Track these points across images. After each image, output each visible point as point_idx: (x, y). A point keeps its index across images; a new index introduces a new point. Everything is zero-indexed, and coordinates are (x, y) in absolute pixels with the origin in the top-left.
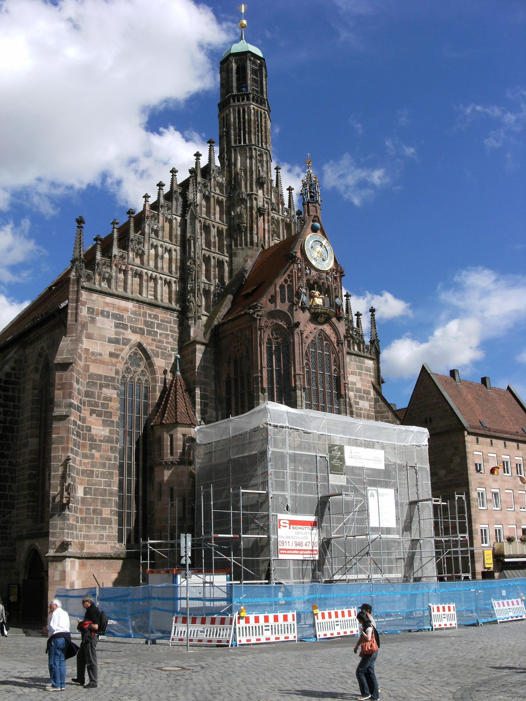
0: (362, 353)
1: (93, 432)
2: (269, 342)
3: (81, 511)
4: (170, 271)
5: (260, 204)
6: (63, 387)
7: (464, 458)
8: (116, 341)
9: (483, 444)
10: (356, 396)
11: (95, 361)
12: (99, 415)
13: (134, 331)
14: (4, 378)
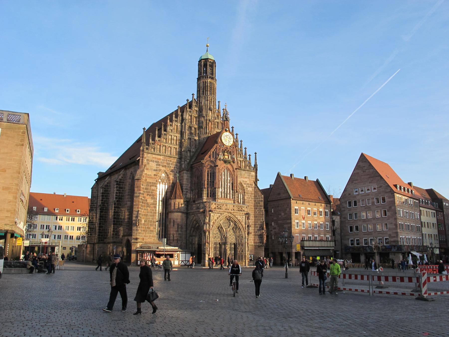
1: (148, 201)
2: (208, 171)
3: (143, 228)
4: (177, 144)
5: (210, 118)
6: (138, 187)
7: (290, 209)
8: (157, 170)
9: (299, 204)
10: (246, 186)
11: (149, 177)
12: (150, 195)
13: (163, 166)
14: (119, 181)
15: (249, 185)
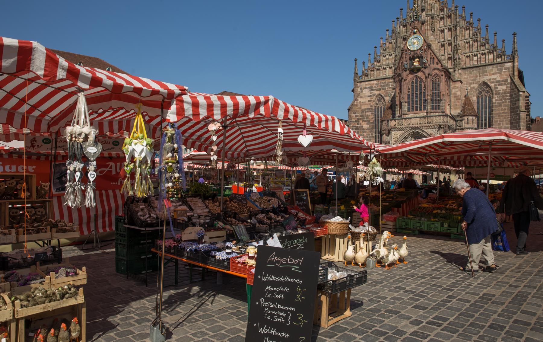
10: (495, 85)
13: (377, 90)
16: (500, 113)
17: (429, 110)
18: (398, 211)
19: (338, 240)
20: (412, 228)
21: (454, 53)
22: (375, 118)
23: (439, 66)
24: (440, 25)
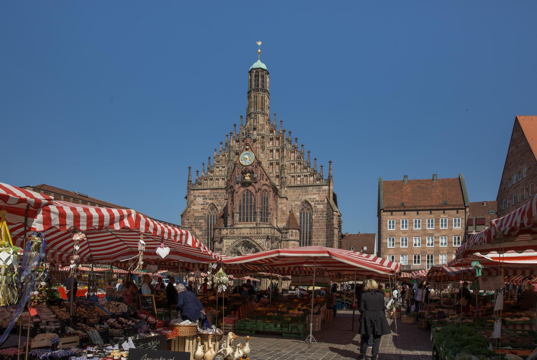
0: (321, 184)
10: (315, 204)
13: (210, 199)
15: (318, 202)
16: (318, 229)
17: (258, 222)
18: (235, 314)
19: (187, 341)
20: (249, 329)
21: (281, 172)
22: (208, 225)
23: (268, 183)
24: (269, 145)
